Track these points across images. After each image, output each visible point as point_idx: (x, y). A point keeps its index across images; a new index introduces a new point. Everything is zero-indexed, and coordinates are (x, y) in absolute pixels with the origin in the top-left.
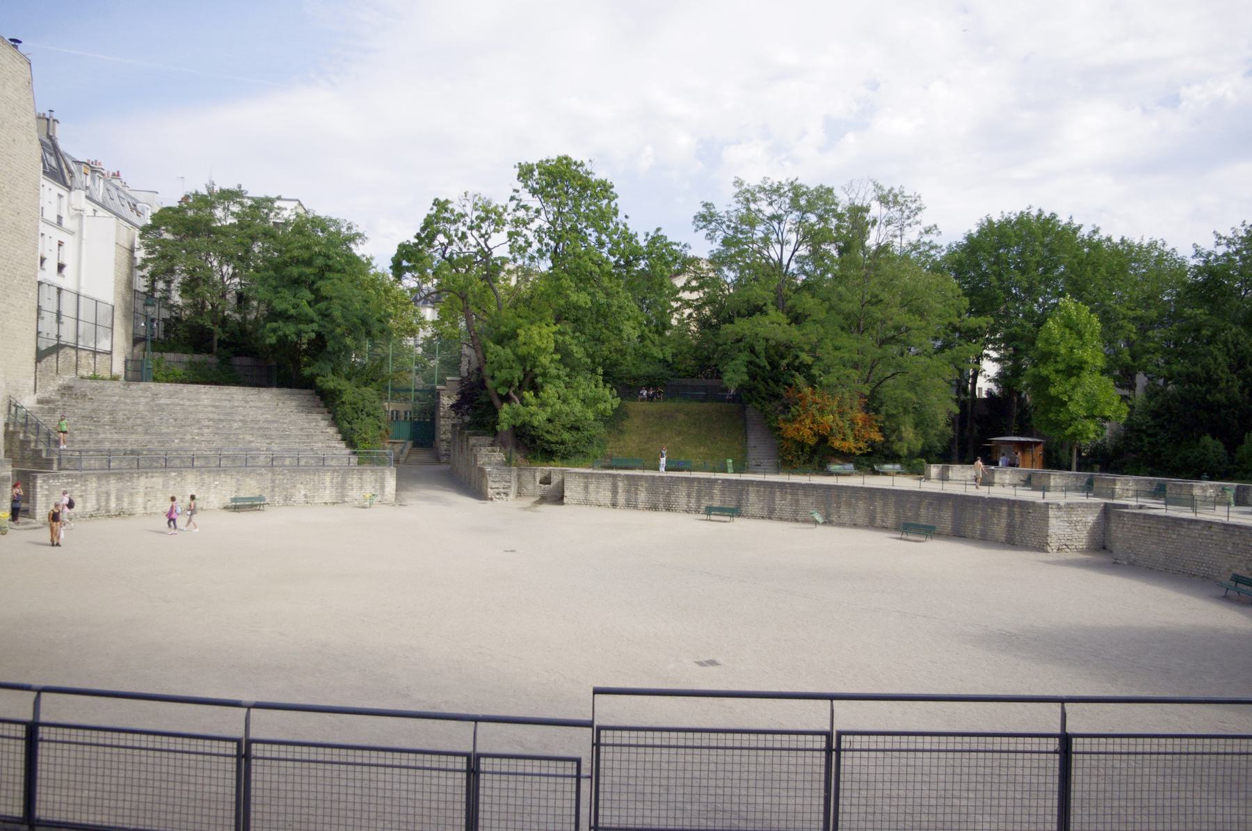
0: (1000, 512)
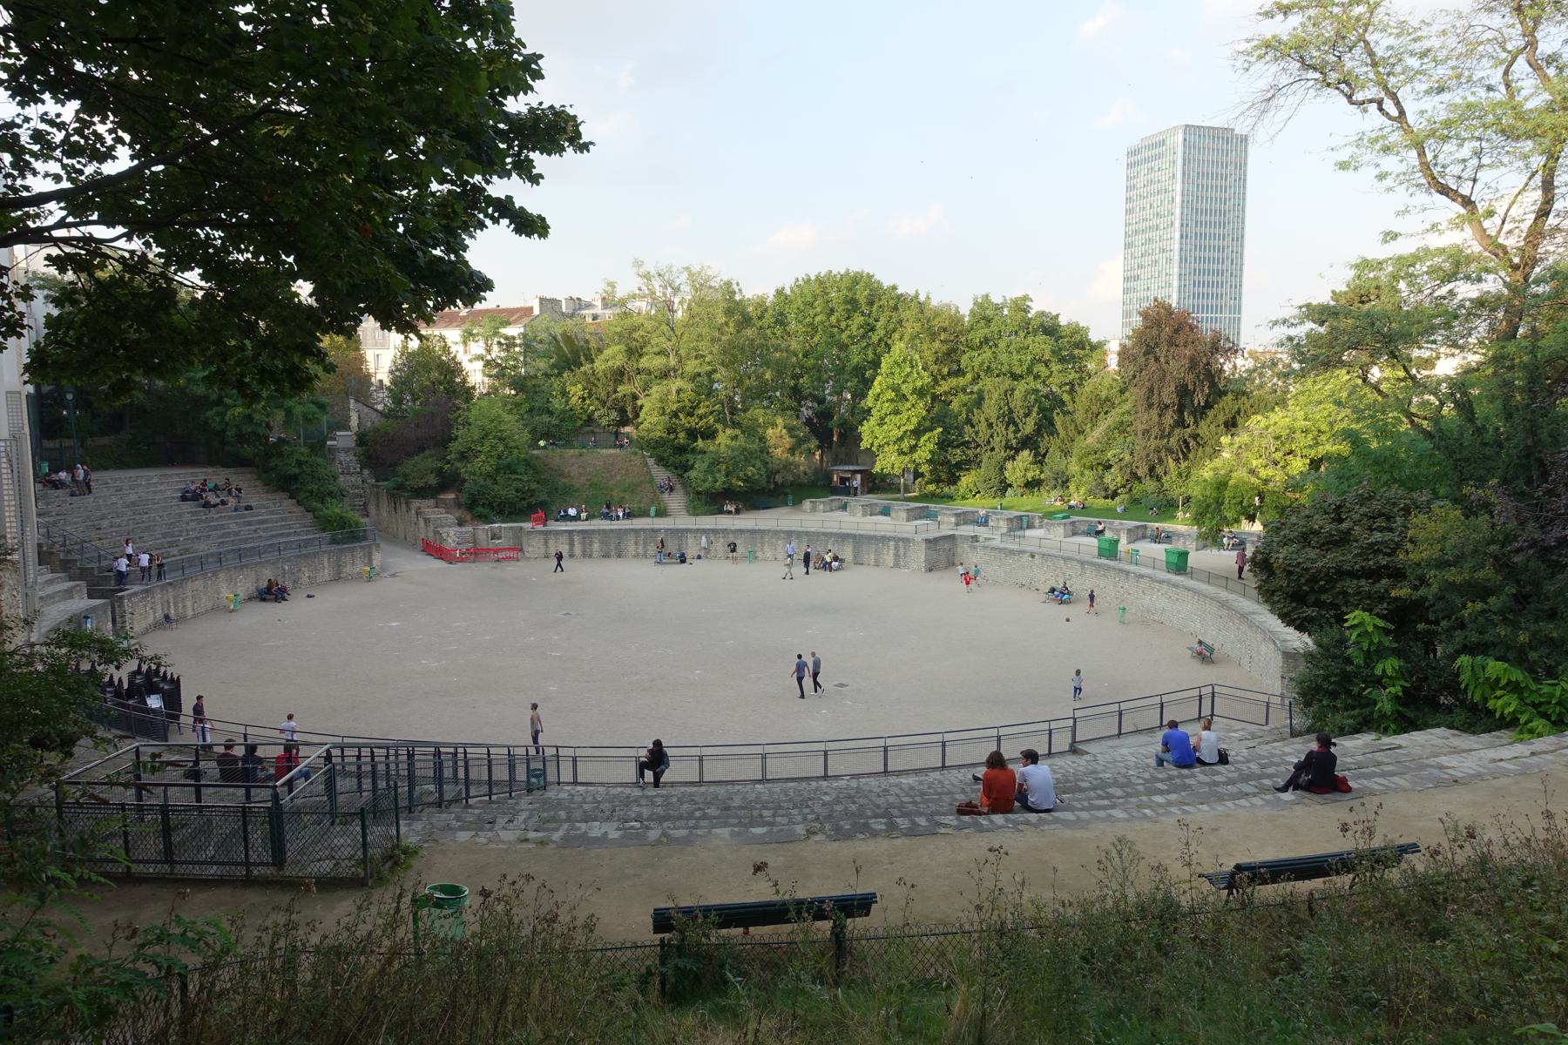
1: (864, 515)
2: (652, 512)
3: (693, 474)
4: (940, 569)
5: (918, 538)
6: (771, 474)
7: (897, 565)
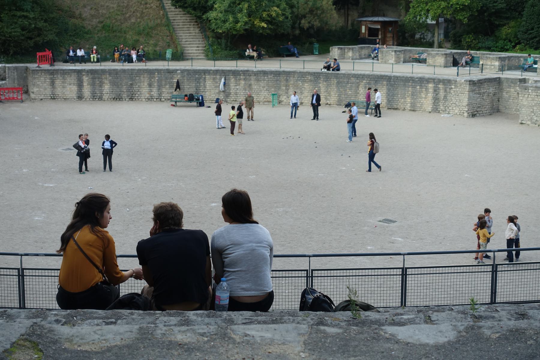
0: (427, 89)
1: (397, 62)
2: (169, 55)
3: (212, 15)
4: (483, 115)
5: (461, 79)
6: (297, 18)
7: (436, 110)
